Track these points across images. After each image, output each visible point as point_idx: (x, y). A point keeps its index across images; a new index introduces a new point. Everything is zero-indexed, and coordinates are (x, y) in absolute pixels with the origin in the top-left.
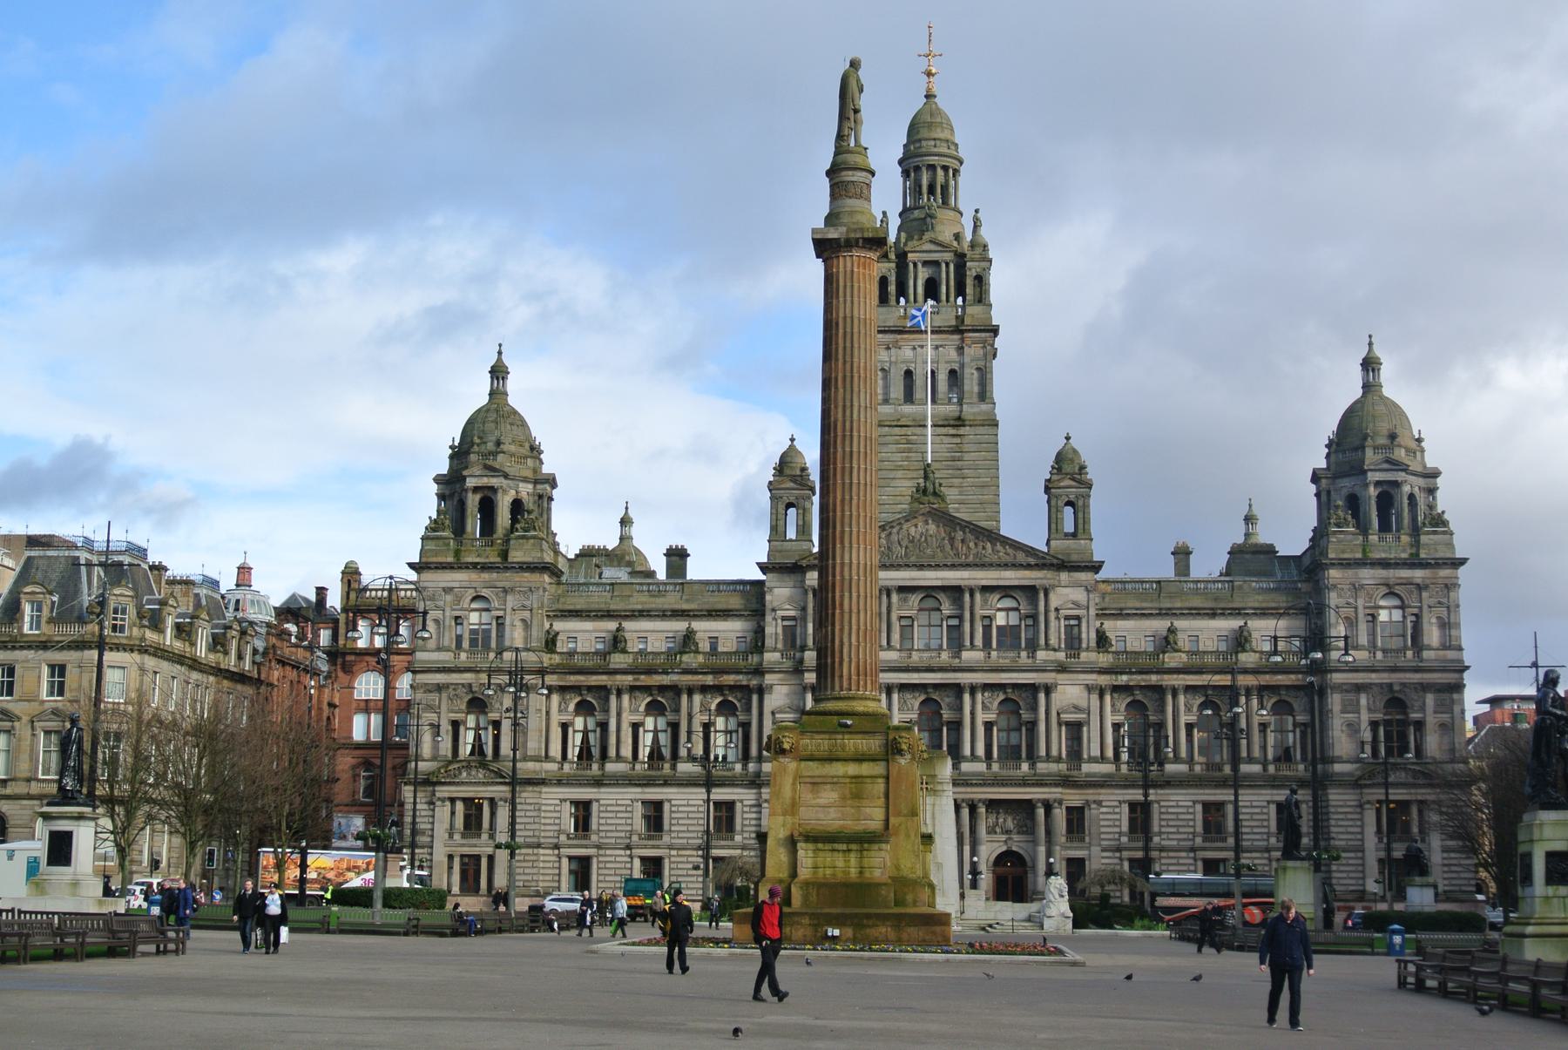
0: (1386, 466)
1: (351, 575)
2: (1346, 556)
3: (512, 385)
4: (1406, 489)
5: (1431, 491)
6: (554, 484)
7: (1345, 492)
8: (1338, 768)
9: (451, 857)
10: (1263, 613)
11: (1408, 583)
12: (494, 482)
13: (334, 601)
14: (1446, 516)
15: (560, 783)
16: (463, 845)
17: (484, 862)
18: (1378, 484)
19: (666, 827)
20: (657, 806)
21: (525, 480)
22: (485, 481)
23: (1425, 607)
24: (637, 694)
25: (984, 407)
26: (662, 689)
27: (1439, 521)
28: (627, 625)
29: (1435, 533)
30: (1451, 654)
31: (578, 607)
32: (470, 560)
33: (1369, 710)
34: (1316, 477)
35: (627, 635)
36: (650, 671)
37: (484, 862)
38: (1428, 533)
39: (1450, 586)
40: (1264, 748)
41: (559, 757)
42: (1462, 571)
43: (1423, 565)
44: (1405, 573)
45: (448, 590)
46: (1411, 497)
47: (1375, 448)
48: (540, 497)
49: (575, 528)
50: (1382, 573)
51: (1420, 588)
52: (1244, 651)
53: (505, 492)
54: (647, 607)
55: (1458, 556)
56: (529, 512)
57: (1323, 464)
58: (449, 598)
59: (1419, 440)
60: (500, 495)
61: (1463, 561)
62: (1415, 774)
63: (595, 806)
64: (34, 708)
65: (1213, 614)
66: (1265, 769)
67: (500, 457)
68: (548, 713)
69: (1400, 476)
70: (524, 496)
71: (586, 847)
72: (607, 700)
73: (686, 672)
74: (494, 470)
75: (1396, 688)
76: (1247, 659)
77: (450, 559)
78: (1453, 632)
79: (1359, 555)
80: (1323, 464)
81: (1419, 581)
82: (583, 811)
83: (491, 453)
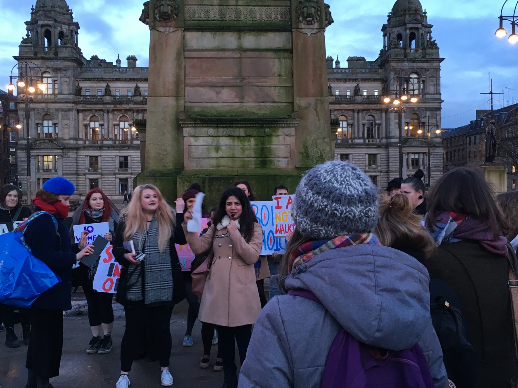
0: (414, 21)
4: (420, 31)
5: (430, 33)
7: (396, 33)
8: (393, 140)
9: (39, 179)
10: (365, 80)
12: (51, 23)
14: (436, 42)
15: (84, 148)
16: (45, 174)
18: (411, 29)
19: (129, 166)
20: (126, 158)
21: (64, 23)
22: (46, 22)
23: (427, 78)
24: (116, 113)
26: (127, 110)
29: (432, 49)
30: (437, 96)
31: (90, 77)
33: (405, 118)
35: (111, 89)
36: (121, 103)
38: (430, 48)
40: (363, 134)
41: (84, 138)
42: (442, 64)
43: (427, 61)
44: (420, 64)
46: (422, 34)
47: (410, 15)
48: (72, 31)
50: (411, 64)
51: (427, 70)
52: (358, 96)
54: (118, 77)
56: (67, 36)
57: (386, 23)
59: (425, 13)
60: (53, 28)
61: (443, 59)
62: (422, 143)
63: (99, 158)
65: (345, 81)
66: (364, 141)
67: (53, 13)
68: (78, 120)
69: (419, 26)
70: (65, 30)
71: (96, 174)
72: (104, 116)
73: (136, 104)
75: (416, 109)
76: (358, 98)
77: (32, 56)
78: (438, 88)
80: (386, 23)
81: (425, 67)
82: (94, 161)
83: (48, 11)
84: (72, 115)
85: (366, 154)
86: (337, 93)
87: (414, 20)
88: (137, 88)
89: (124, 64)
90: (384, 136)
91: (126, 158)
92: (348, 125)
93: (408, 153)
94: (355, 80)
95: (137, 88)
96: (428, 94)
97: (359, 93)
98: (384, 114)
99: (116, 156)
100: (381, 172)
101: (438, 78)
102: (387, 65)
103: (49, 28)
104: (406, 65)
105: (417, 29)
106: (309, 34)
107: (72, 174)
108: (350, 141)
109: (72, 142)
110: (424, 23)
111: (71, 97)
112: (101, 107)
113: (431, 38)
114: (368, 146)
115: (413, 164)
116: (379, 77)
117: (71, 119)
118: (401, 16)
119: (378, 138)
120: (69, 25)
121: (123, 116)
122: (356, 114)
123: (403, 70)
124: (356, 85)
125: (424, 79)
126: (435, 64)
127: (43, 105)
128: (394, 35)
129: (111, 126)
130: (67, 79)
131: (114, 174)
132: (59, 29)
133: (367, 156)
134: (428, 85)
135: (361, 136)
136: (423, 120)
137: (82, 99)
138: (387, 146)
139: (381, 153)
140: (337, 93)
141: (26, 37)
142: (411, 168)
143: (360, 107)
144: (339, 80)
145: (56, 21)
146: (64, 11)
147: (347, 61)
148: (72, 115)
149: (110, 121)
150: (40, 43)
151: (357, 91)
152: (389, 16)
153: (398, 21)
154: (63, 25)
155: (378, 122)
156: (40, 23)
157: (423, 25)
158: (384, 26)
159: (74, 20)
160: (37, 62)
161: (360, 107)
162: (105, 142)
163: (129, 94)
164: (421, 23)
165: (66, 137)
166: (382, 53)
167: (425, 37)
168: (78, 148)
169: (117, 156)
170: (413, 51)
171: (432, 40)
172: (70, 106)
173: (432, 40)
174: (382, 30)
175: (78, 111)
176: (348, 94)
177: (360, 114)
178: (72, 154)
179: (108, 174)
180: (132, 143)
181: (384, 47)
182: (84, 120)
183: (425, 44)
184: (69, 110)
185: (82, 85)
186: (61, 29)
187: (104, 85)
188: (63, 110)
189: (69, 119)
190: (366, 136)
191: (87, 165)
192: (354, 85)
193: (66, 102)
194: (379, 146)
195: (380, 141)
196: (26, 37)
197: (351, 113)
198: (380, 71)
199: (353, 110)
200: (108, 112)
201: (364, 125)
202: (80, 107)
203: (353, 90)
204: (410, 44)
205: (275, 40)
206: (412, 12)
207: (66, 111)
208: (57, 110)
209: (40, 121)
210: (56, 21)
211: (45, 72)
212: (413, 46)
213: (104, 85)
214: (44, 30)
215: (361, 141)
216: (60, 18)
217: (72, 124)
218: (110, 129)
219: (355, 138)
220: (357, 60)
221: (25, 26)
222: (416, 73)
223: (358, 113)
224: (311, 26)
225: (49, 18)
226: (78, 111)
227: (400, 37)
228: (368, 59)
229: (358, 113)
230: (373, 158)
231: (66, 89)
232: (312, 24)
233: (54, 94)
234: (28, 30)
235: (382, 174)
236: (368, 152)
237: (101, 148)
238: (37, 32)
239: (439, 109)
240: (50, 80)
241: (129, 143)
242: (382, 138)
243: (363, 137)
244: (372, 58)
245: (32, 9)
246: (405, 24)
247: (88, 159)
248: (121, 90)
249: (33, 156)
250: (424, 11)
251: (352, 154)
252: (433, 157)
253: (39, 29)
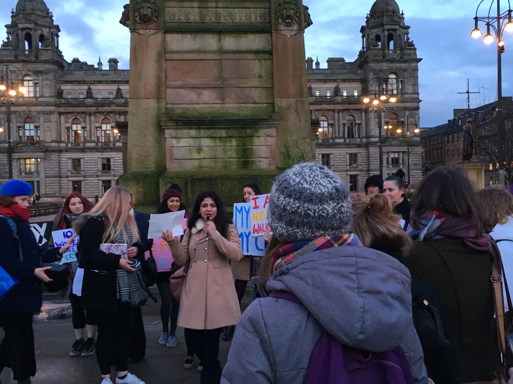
0: (392, 23)
4: (398, 32)
5: (407, 34)
7: (375, 34)
8: (373, 140)
10: (344, 81)
11: (400, 69)
12: (30, 26)
14: (413, 43)
15: (67, 151)
16: (26, 177)
17: (36, 184)
18: (388, 30)
19: (112, 168)
20: (109, 160)
21: (45, 27)
22: (27, 25)
23: (406, 78)
24: (98, 115)
26: (109, 113)
27: (411, 45)
28: (93, 87)
29: (410, 49)
30: (415, 96)
31: (71, 80)
33: (385, 117)
35: (93, 92)
36: (103, 105)
37: (36, 184)
39: (416, 69)
40: (344, 134)
41: (66, 141)
42: (420, 64)
43: (405, 62)
44: (398, 65)
46: (400, 35)
47: (387, 16)
48: (52, 34)
51: (405, 70)
52: (338, 96)
54: (100, 80)
55: (418, 58)
56: (48, 39)
57: (365, 24)
59: (403, 14)
61: (420, 60)
62: (402, 142)
63: (82, 161)
65: (325, 81)
66: (345, 141)
67: (33, 16)
68: (60, 123)
69: (397, 27)
70: (45, 33)
71: (79, 177)
72: (85, 118)
73: (117, 106)
75: (395, 109)
76: (339, 99)
77: (13, 59)
80: (365, 24)
81: (403, 68)
82: (76, 163)
83: (28, 14)
84: (54, 117)
85: (346, 153)
86: (317, 94)
87: (392, 21)
88: (119, 91)
89: (106, 67)
90: (364, 135)
91: (109, 160)
92: (328, 125)
93: (388, 152)
94: (335, 81)
95: (119, 91)
96: (407, 93)
97: (339, 94)
98: (363, 114)
99: (98, 158)
100: (362, 171)
101: (416, 78)
102: (366, 66)
103: (29, 31)
104: (385, 66)
105: (395, 30)
106: (289, 36)
107: (54, 177)
108: (331, 141)
109: (54, 144)
110: (402, 24)
111: (52, 100)
112: (83, 109)
113: (408, 39)
114: (348, 145)
115: (393, 163)
116: (358, 78)
117: (53, 122)
118: (379, 17)
119: (359, 137)
120: (50, 28)
121: (106, 118)
122: (336, 114)
123: (381, 71)
124: (336, 85)
125: (402, 79)
126: (413, 64)
127: (24, 108)
128: (373, 37)
129: (93, 128)
130: (48, 82)
131: (97, 176)
132: (40, 31)
133: (348, 155)
134: (406, 85)
135: (341, 135)
136: (402, 119)
137: (63, 101)
138: (367, 146)
139: (361, 152)
140: (317, 94)
141: (6, 40)
142: (391, 166)
143: (341, 107)
144: (319, 81)
145: (36, 24)
146: (44, 14)
147: (327, 62)
148: (54, 117)
149: (93, 124)
150: (20, 46)
151: (337, 92)
152: (367, 18)
153: (377, 22)
154: (43, 28)
155: (358, 122)
156: (20, 26)
157: (400, 27)
158: (362, 27)
159: (55, 23)
160: (19, 65)
161: (341, 107)
162: (88, 145)
163: (111, 96)
164: (399, 25)
165: (48, 139)
166: (361, 53)
167: (402, 38)
168: (60, 151)
169: (100, 158)
170: (391, 52)
171: (410, 41)
172: (52, 108)
173: (410, 41)
174: (361, 31)
175: (60, 114)
176: (328, 94)
177: (341, 114)
178: (54, 156)
179: (91, 176)
180: (114, 145)
181: (363, 48)
182: (66, 122)
183: (403, 45)
184: (51, 113)
185: (63, 87)
186: (42, 31)
187: (86, 87)
188: (44, 113)
189: (51, 122)
190: (346, 136)
191: (69, 167)
192: (334, 85)
193: (48, 105)
194: (359, 146)
195: (360, 141)
196: (6, 40)
197: (331, 113)
198: (359, 71)
199: (333, 111)
200: (90, 114)
201: (344, 125)
202: (62, 110)
203: (333, 90)
204: (389, 45)
205: (255, 42)
206: (390, 14)
207: (47, 114)
208: (39, 113)
209: (22, 124)
210: (36, 24)
211: (26, 75)
212: (391, 46)
213: (86, 87)
214: (24, 33)
215: (342, 141)
216: (40, 21)
217: (54, 126)
218: (92, 132)
219: (336, 138)
220: (337, 61)
221: (6, 29)
222: (395, 73)
223: (338, 113)
224: (291, 28)
225: (29, 21)
226: (60, 114)
227: (378, 38)
228: (347, 60)
229: (338, 113)
230: (353, 157)
231: (47, 92)
232: (291, 26)
233: (35, 97)
234: (8, 33)
235: (362, 173)
236: (349, 152)
237: (83, 150)
238: (17, 35)
239: (417, 108)
240: (31, 83)
241: (111, 145)
242: (362, 138)
243: (344, 137)
244: (350, 59)
245: (12, 12)
246: (383, 25)
247: (70, 161)
248: (103, 92)
249: (15, 159)
250: (401, 13)
251: (333, 154)
252: (412, 156)
253: (19, 32)
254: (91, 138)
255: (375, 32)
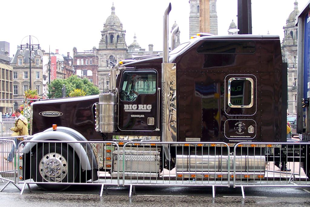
1: (75, 50)
2: (290, 44)
3: (116, 11)
6: (125, 31)
7: (290, 31)
12: (114, 32)
13: (72, 55)
21: (120, 31)
25: (214, 13)
32: (109, 48)
34: (284, 28)
45: (105, 55)
48: (123, 34)
49: (129, 41)
53: (116, 34)
58: (105, 56)
60: (115, 34)
64: (22, 81)
74: (113, 29)
77: (105, 48)
79: (293, 44)
89: (147, 50)
128: (289, 32)
156: (109, 32)
186: (118, 34)
210: (116, 30)
214: (110, 35)
227: (292, 33)
234: (103, 35)
238: (107, 36)
253: (108, 35)
254: (141, 87)
255: (290, 29)
